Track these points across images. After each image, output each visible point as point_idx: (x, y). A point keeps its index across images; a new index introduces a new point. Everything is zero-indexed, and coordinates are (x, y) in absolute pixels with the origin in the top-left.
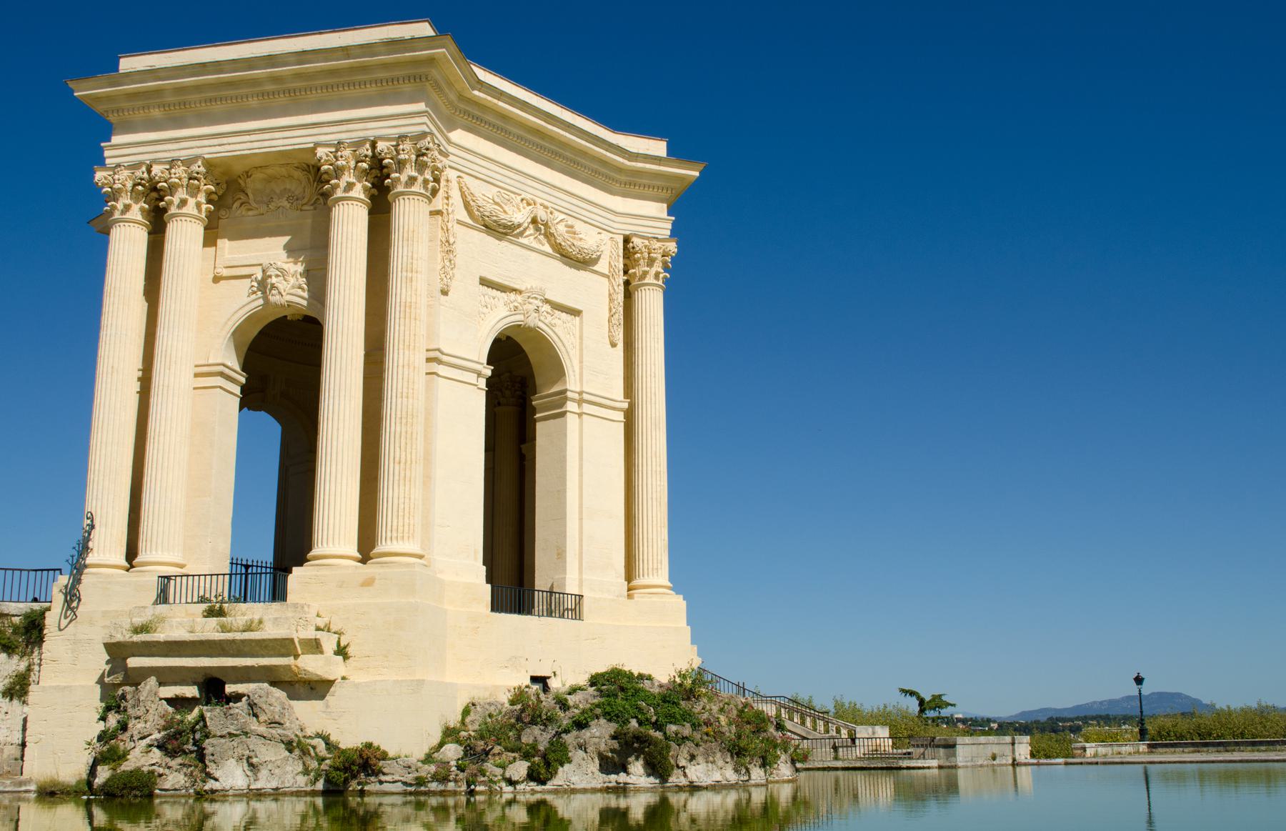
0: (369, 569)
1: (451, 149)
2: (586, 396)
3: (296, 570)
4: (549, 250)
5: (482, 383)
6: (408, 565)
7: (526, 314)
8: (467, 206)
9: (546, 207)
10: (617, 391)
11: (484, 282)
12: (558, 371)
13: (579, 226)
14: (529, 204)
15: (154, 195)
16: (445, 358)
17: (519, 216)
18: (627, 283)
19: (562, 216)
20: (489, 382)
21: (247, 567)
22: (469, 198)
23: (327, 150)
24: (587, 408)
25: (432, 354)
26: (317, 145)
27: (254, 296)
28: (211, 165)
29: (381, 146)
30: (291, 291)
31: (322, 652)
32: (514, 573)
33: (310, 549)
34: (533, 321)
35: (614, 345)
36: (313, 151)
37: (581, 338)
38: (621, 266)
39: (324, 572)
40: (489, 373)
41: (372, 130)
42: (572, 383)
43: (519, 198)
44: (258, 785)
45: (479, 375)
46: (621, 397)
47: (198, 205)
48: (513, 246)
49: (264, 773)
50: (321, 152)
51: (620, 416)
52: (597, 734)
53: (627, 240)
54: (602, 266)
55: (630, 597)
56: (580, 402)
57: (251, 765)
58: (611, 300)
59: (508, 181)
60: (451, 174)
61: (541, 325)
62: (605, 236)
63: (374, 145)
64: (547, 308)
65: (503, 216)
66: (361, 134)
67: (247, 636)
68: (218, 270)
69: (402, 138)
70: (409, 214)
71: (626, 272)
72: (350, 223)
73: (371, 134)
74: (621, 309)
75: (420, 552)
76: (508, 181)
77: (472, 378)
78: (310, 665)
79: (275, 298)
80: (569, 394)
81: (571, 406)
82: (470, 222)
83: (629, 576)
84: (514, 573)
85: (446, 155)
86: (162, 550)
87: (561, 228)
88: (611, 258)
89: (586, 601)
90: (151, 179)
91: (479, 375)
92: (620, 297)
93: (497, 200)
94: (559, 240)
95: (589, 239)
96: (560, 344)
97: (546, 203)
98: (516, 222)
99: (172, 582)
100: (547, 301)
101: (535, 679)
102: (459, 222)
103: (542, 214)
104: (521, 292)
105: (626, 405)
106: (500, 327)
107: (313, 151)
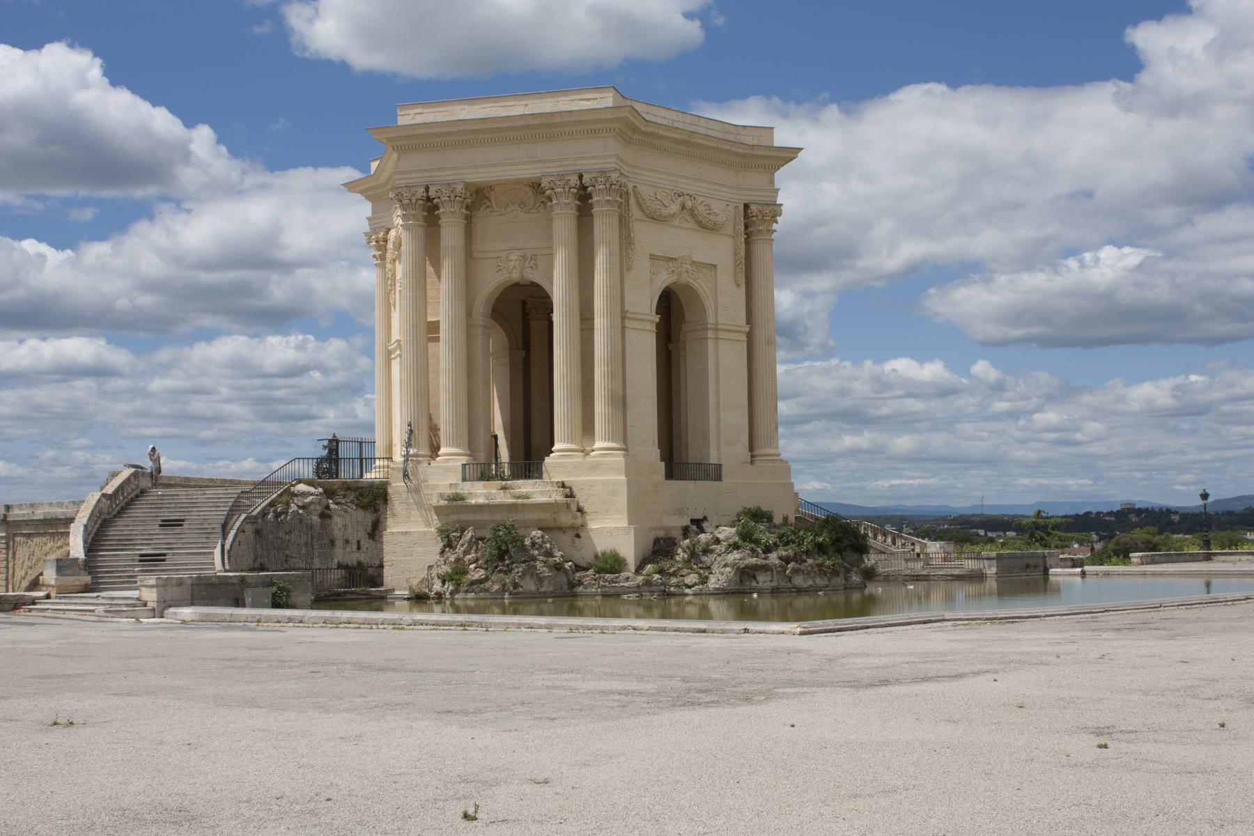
3: (547, 460)
4: (692, 225)
7: (680, 274)
8: (639, 205)
11: (652, 257)
18: (747, 242)
20: (658, 326)
24: (721, 335)
28: (467, 186)
29: (586, 179)
33: (552, 445)
34: (685, 278)
35: (738, 285)
37: (716, 285)
41: (583, 165)
42: (711, 320)
44: (543, 590)
45: (652, 322)
49: (546, 583)
51: (744, 338)
53: (746, 206)
55: (752, 463)
60: (630, 186)
63: (581, 177)
67: (525, 501)
71: (746, 227)
78: (565, 519)
81: (710, 334)
83: (751, 449)
87: (701, 209)
89: (724, 468)
91: (652, 322)
92: (743, 253)
94: (700, 218)
101: (693, 521)
103: (689, 204)
107: (540, 178)
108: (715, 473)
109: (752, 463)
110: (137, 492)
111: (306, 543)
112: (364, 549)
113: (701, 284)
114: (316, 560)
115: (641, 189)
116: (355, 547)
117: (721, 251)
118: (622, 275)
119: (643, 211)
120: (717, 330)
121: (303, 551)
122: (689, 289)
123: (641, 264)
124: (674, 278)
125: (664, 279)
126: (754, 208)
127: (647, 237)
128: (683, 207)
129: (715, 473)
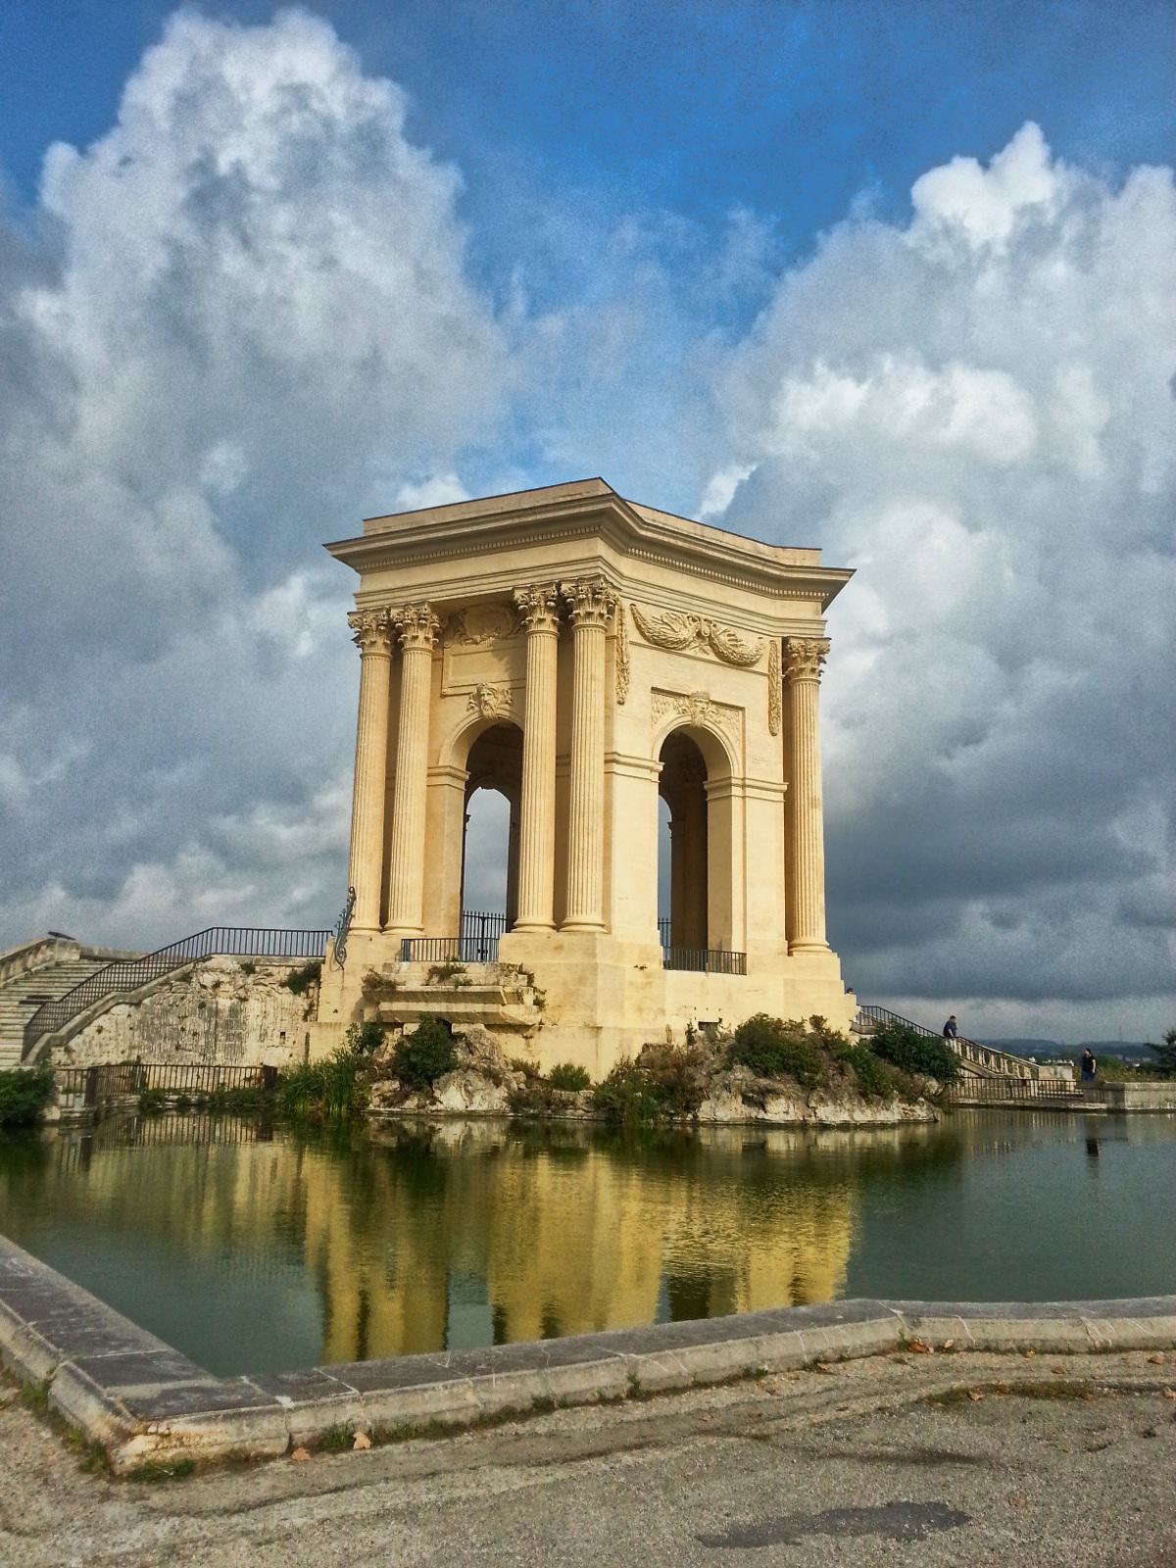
0: (559, 937)
1: (624, 583)
2: (748, 782)
4: (712, 657)
5: (655, 777)
6: (589, 933)
7: (693, 715)
8: (638, 627)
9: (711, 622)
10: (776, 774)
11: (654, 690)
12: (723, 759)
13: (740, 634)
14: (694, 621)
15: (394, 632)
16: (622, 759)
17: (687, 633)
18: (785, 681)
19: (725, 627)
21: (483, 919)
22: (640, 623)
23: (522, 592)
24: (749, 792)
25: (610, 757)
26: (515, 588)
27: (471, 711)
28: (436, 607)
30: (497, 707)
31: (523, 1003)
32: (691, 933)
34: (699, 720)
35: (774, 734)
36: (512, 591)
37: (744, 731)
38: (780, 665)
39: (525, 937)
40: (661, 768)
42: (736, 772)
43: (686, 616)
45: (652, 770)
46: (782, 782)
47: (427, 639)
48: (681, 658)
49: (477, 1098)
50: (518, 594)
51: (780, 797)
52: (740, 1077)
53: (785, 641)
54: (762, 666)
55: (790, 954)
56: (744, 786)
57: (467, 1091)
58: (771, 697)
59: (675, 603)
60: (626, 604)
61: (706, 723)
62: (767, 640)
64: (713, 707)
65: (670, 634)
66: (548, 578)
68: (445, 690)
69: (581, 579)
70: (591, 644)
71: (785, 668)
72: (543, 649)
73: (556, 578)
74: (780, 704)
75: (602, 922)
76: (675, 603)
77: (646, 774)
78: (513, 1012)
79: (488, 713)
80: (733, 781)
81: (736, 791)
82: (647, 643)
84: (691, 933)
85: (620, 590)
86: (407, 920)
87: (724, 638)
88: (768, 659)
90: (390, 620)
93: (665, 621)
94: (721, 649)
95: (749, 643)
96: (724, 738)
97: (710, 618)
98: (682, 638)
99: (412, 943)
100: (713, 702)
102: (632, 643)
103: (705, 629)
104: (688, 696)
105: (785, 788)
106: (671, 728)
108: (735, 964)
109: (790, 954)
110: (52, 964)
111: (207, 1033)
112: (289, 1043)
113: (724, 728)
114: (219, 1055)
115: (640, 607)
116: (277, 1040)
117: (754, 692)
118: (608, 707)
119: (642, 634)
120: (744, 786)
121: (202, 1042)
122: (704, 732)
123: (638, 696)
124: (686, 719)
125: (671, 718)
126: (794, 642)
127: (647, 666)
128: (699, 634)
129: (735, 964)
